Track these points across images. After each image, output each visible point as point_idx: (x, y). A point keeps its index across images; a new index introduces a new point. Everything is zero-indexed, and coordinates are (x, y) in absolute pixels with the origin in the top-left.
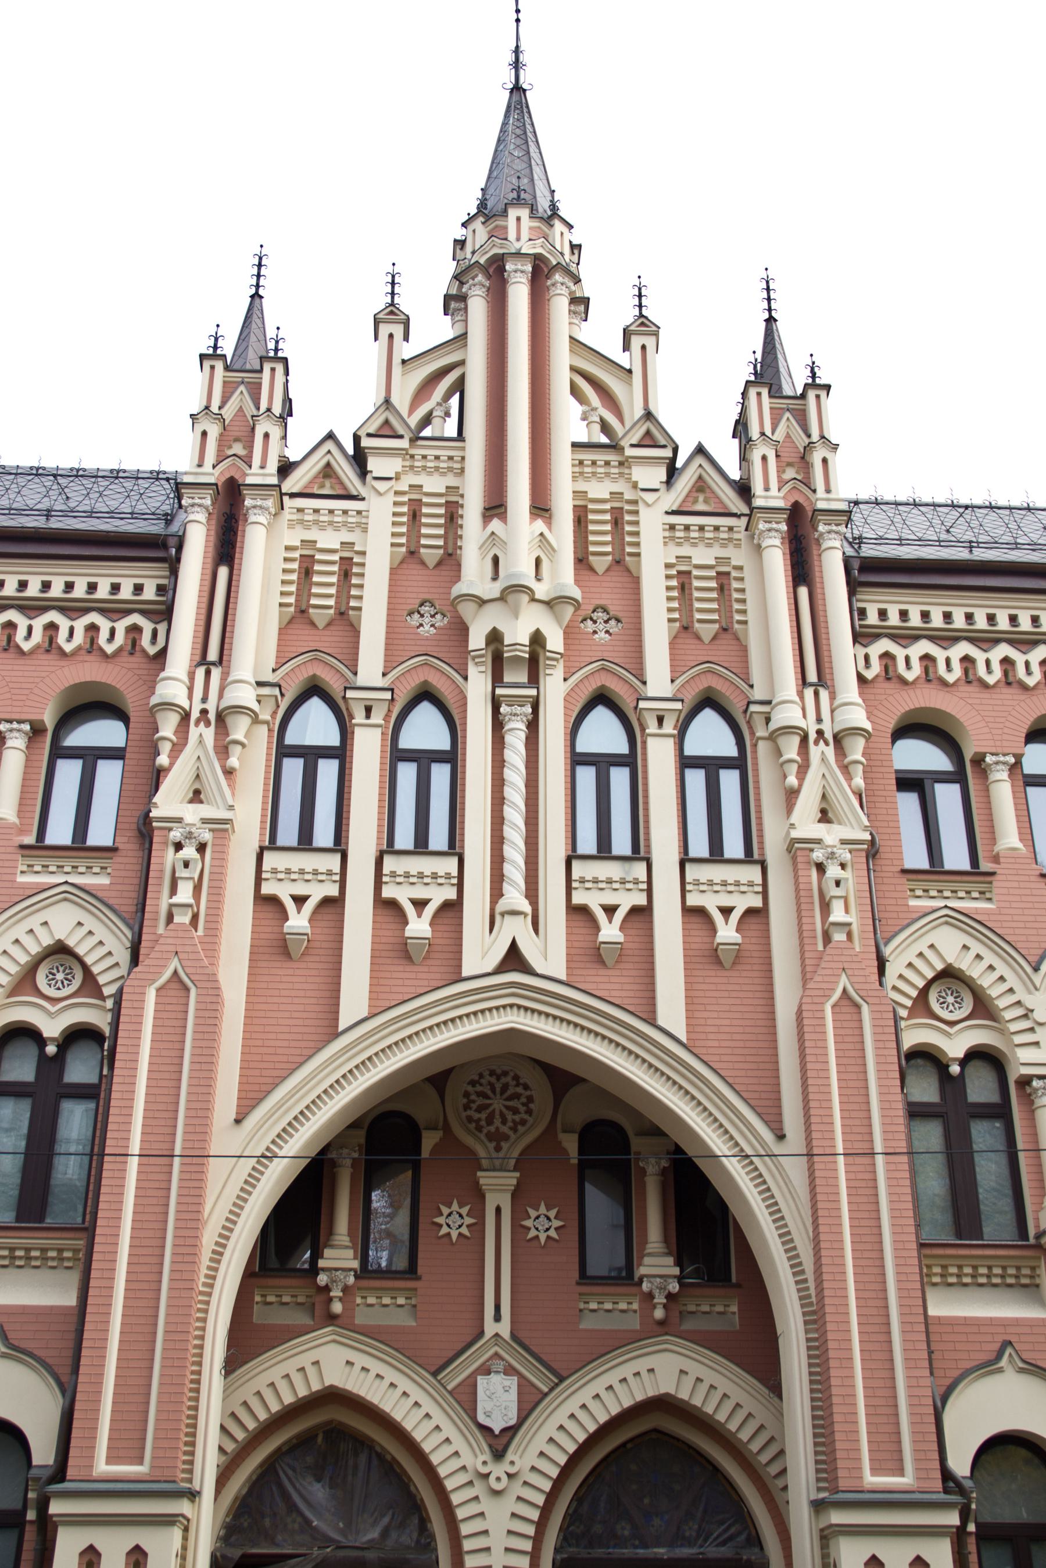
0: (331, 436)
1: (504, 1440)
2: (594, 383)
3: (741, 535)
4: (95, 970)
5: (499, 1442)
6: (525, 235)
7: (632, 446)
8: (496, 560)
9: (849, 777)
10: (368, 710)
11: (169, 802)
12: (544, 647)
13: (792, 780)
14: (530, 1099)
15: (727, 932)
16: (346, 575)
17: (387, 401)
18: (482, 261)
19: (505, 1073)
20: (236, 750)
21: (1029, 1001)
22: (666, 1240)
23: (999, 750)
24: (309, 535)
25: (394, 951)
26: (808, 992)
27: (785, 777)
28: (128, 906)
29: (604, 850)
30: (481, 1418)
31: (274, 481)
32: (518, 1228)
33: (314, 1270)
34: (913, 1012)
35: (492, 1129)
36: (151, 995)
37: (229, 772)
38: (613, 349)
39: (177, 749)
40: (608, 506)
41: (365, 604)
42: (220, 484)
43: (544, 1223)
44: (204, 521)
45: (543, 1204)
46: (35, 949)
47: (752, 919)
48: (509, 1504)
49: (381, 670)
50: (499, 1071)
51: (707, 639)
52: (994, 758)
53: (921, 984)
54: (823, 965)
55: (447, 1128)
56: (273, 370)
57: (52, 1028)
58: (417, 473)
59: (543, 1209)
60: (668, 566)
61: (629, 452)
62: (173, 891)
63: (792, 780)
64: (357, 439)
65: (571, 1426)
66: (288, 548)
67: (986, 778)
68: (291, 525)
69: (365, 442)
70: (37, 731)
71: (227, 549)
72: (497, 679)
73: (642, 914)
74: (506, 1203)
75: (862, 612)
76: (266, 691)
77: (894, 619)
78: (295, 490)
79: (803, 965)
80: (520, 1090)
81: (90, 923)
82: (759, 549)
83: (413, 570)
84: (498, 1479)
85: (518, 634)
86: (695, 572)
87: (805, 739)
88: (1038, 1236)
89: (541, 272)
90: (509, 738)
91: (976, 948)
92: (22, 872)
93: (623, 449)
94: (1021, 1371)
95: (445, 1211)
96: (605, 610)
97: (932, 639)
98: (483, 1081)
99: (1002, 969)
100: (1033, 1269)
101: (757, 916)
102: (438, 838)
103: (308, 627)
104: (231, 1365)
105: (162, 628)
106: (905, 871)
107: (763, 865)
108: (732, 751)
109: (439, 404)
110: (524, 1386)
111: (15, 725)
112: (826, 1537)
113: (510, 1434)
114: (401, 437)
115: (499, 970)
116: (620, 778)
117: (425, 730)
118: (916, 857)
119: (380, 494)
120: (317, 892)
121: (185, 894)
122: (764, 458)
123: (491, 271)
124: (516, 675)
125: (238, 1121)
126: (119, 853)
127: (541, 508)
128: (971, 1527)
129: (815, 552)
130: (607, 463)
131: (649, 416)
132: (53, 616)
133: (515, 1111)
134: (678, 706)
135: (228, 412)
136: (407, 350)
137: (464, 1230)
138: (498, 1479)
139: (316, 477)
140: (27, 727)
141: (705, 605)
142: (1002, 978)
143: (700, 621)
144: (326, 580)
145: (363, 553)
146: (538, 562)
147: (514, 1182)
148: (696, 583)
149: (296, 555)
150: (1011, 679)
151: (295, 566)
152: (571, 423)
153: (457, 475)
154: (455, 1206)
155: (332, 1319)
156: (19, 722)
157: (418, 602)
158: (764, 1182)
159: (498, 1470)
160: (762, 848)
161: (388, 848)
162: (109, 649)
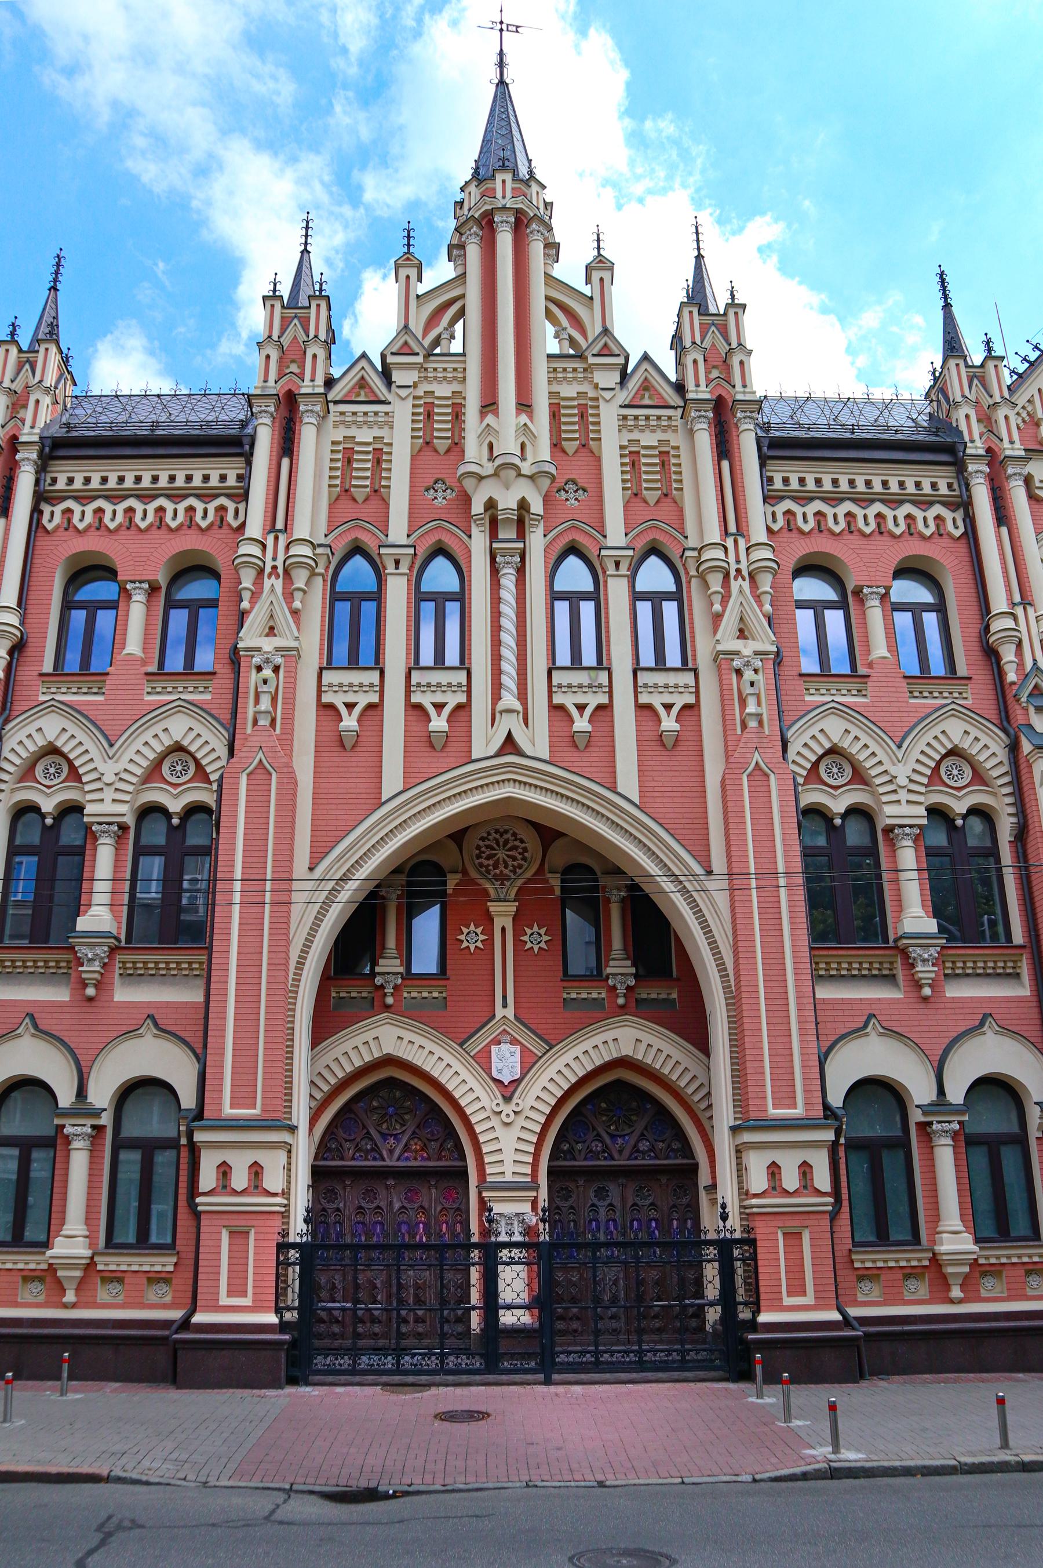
0: (364, 356)
1: (512, 1089)
2: (563, 307)
3: (678, 422)
4: (204, 762)
5: (508, 1091)
6: (509, 194)
7: (594, 355)
8: (491, 446)
9: (761, 606)
10: (397, 563)
11: (250, 637)
12: (528, 511)
13: (717, 607)
14: (525, 850)
15: (669, 723)
16: (378, 462)
17: (406, 327)
18: (476, 216)
19: (506, 832)
20: (298, 595)
21: (893, 771)
22: (625, 949)
23: (874, 584)
24: (350, 433)
25: (423, 744)
26: (730, 766)
27: (712, 605)
28: (226, 716)
29: (576, 662)
30: (495, 1074)
31: (322, 390)
32: (518, 943)
33: (373, 974)
34: (807, 780)
35: (497, 871)
36: (244, 780)
37: (295, 613)
38: (578, 281)
39: (255, 596)
40: (575, 403)
41: (393, 483)
42: (281, 395)
43: (537, 938)
44: (270, 423)
46: (159, 749)
47: (687, 713)
48: (516, 1132)
49: (406, 532)
50: (502, 830)
51: (652, 503)
52: (870, 590)
53: (814, 758)
54: (741, 745)
55: (465, 872)
56: (318, 306)
57: (175, 806)
58: (430, 382)
59: (536, 928)
60: (622, 447)
61: (592, 360)
62: (257, 702)
63: (717, 607)
64: (383, 357)
65: (558, 1079)
66: (333, 443)
67: (864, 605)
68: (335, 426)
69: (390, 359)
70: (153, 589)
71: (287, 445)
72: (494, 535)
73: (604, 710)
75: (770, 480)
76: (319, 551)
77: (794, 485)
78: (337, 399)
79: (726, 746)
80: (517, 843)
81: (198, 728)
82: (691, 433)
83: (428, 455)
84: (508, 1115)
85: (508, 501)
86: (643, 452)
87: (727, 575)
88: (896, 940)
89: (521, 223)
90: (503, 581)
91: (855, 731)
92: (148, 693)
93: (587, 358)
94: (881, 1034)
95: (465, 930)
96: (575, 483)
97: (823, 499)
98: (490, 837)
99: (873, 747)
100: (891, 963)
101: (691, 710)
102: (452, 657)
103: (351, 502)
104: (316, 1040)
105: (242, 507)
106: (801, 675)
107: (695, 671)
108: (672, 588)
109: (446, 329)
110: (525, 1052)
111: (137, 585)
112: (739, 1151)
113: (516, 1084)
114: (417, 354)
115: (499, 754)
116: (587, 609)
117: (441, 576)
118: (810, 665)
119: (403, 399)
120: (363, 700)
121: (265, 704)
122: (695, 362)
123: (483, 223)
124: (507, 533)
125: (311, 869)
126: (217, 676)
127: (524, 405)
128: (842, 1141)
129: (734, 434)
130: (575, 370)
131: (606, 331)
132: (161, 502)
133: (514, 859)
134: (631, 553)
135: (286, 341)
136: (422, 289)
137: (480, 944)
138: (508, 1115)
139: (353, 388)
140: (146, 586)
141: (650, 476)
142: (873, 754)
143: (647, 489)
144: (363, 466)
145: (391, 444)
146: (523, 446)
147: (515, 909)
148: (643, 460)
149: (341, 448)
150: (883, 530)
151: (340, 456)
152: (548, 341)
153: (460, 382)
155: (387, 1008)
156: (140, 582)
157: (432, 480)
158: (698, 905)
159: (508, 1109)
160: (694, 660)
161: (414, 665)
162: (204, 524)
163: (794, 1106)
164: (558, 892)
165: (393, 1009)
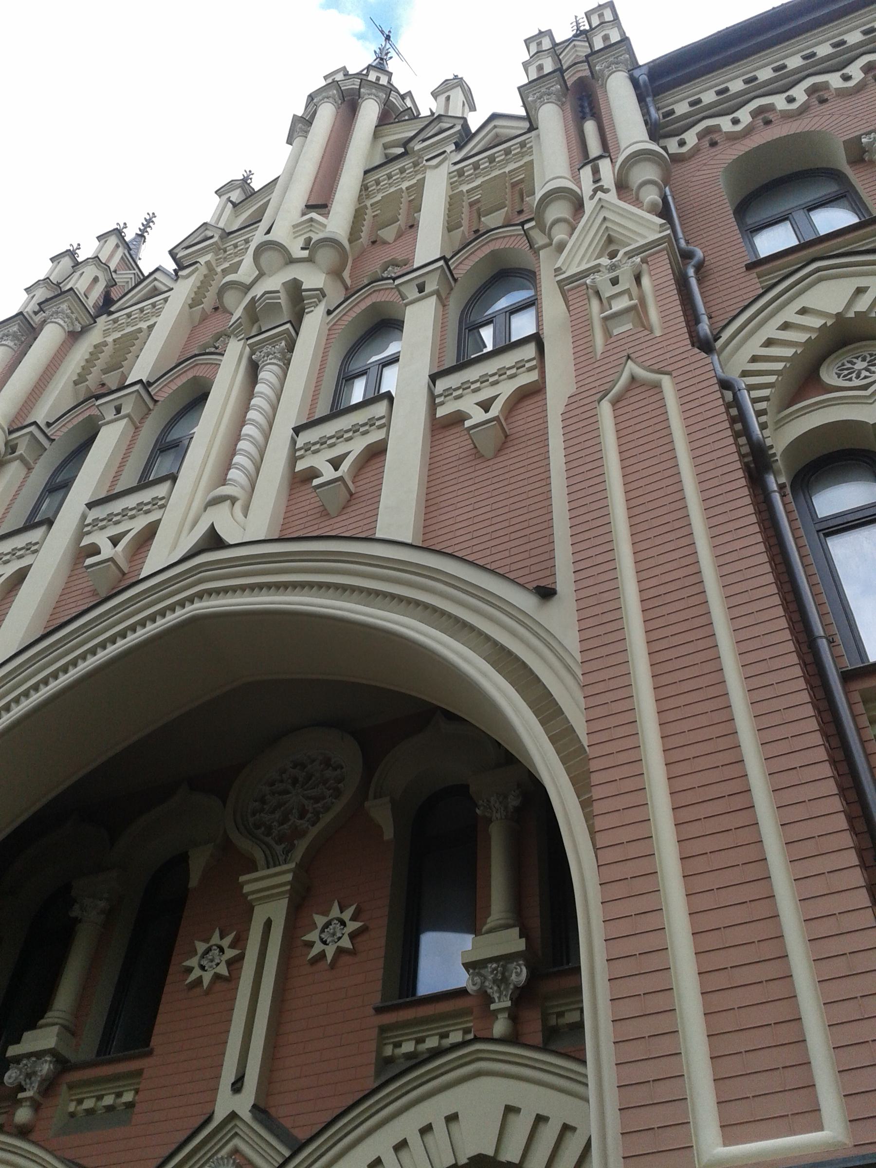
45: (336, 904)
59: (335, 912)
74: (276, 911)
95: (201, 947)
154: (215, 939)
163: (812, 1117)
164: (389, 834)
165: (33, 1137)
